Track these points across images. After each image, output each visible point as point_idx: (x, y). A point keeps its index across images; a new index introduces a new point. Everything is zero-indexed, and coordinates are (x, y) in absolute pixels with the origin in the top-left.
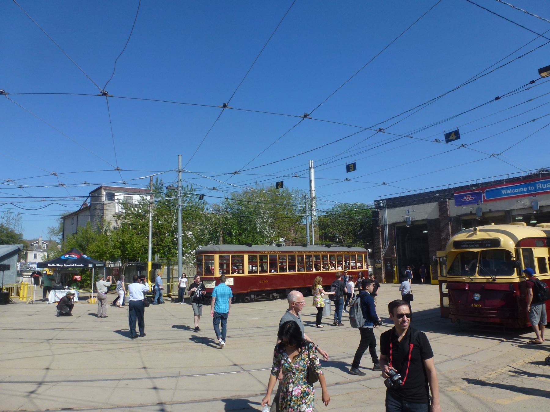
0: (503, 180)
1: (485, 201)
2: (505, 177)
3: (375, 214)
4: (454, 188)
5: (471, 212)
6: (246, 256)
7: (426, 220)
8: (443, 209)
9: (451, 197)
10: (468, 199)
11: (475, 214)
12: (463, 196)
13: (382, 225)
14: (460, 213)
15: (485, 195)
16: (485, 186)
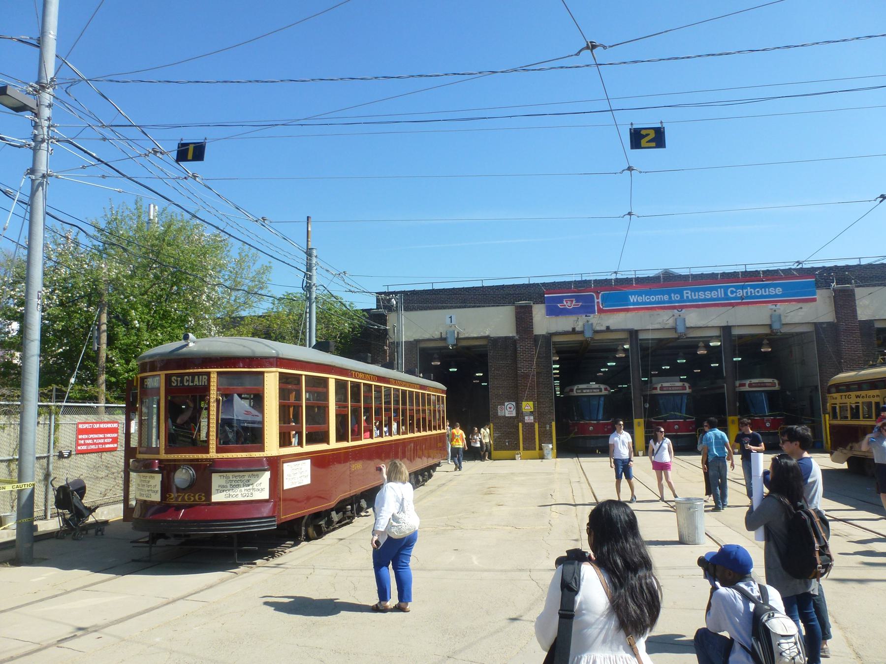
0: (590, 281)
1: (601, 311)
2: (741, 269)
4: (544, 284)
5: (574, 329)
8: (523, 319)
9: (540, 300)
10: (567, 304)
11: (582, 332)
12: (560, 300)
13: (393, 343)
14: (553, 330)
15: (600, 300)
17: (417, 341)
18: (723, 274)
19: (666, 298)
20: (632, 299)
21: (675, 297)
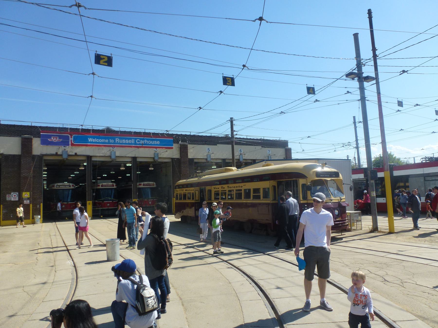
0: (67, 128)
1: (72, 145)
2: (143, 131)
4: (40, 127)
5: (57, 153)
6: (235, 199)
10: (53, 139)
11: (61, 155)
12: (50, 137)
14: (44, 152)
15: (72, 139)
16: (74, 131)
18: (153, 134)
19: (107, 141)
20: (90, 140)
21: (112, 141)
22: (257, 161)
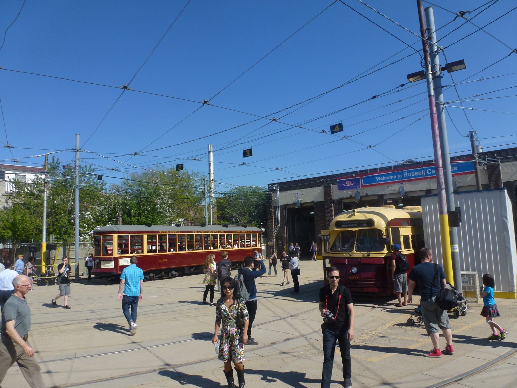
1: (363, 186)
2: (379, 166)
3: (269, 196)
4: (337, 175)
5: (351, 196)
6: (145, 236)
7: (313, 202)
8: (327, 193)
10: (348, 184)
11: (354, 198)
12: (344, 182)
13: (275, 207)
14: (341, 197)
15: (362, 181)
16: (364, 173)
17: (285, 205)
19: (395, 177)
20: (378, 179)
21: (400, 176)
22: (433, 193)
